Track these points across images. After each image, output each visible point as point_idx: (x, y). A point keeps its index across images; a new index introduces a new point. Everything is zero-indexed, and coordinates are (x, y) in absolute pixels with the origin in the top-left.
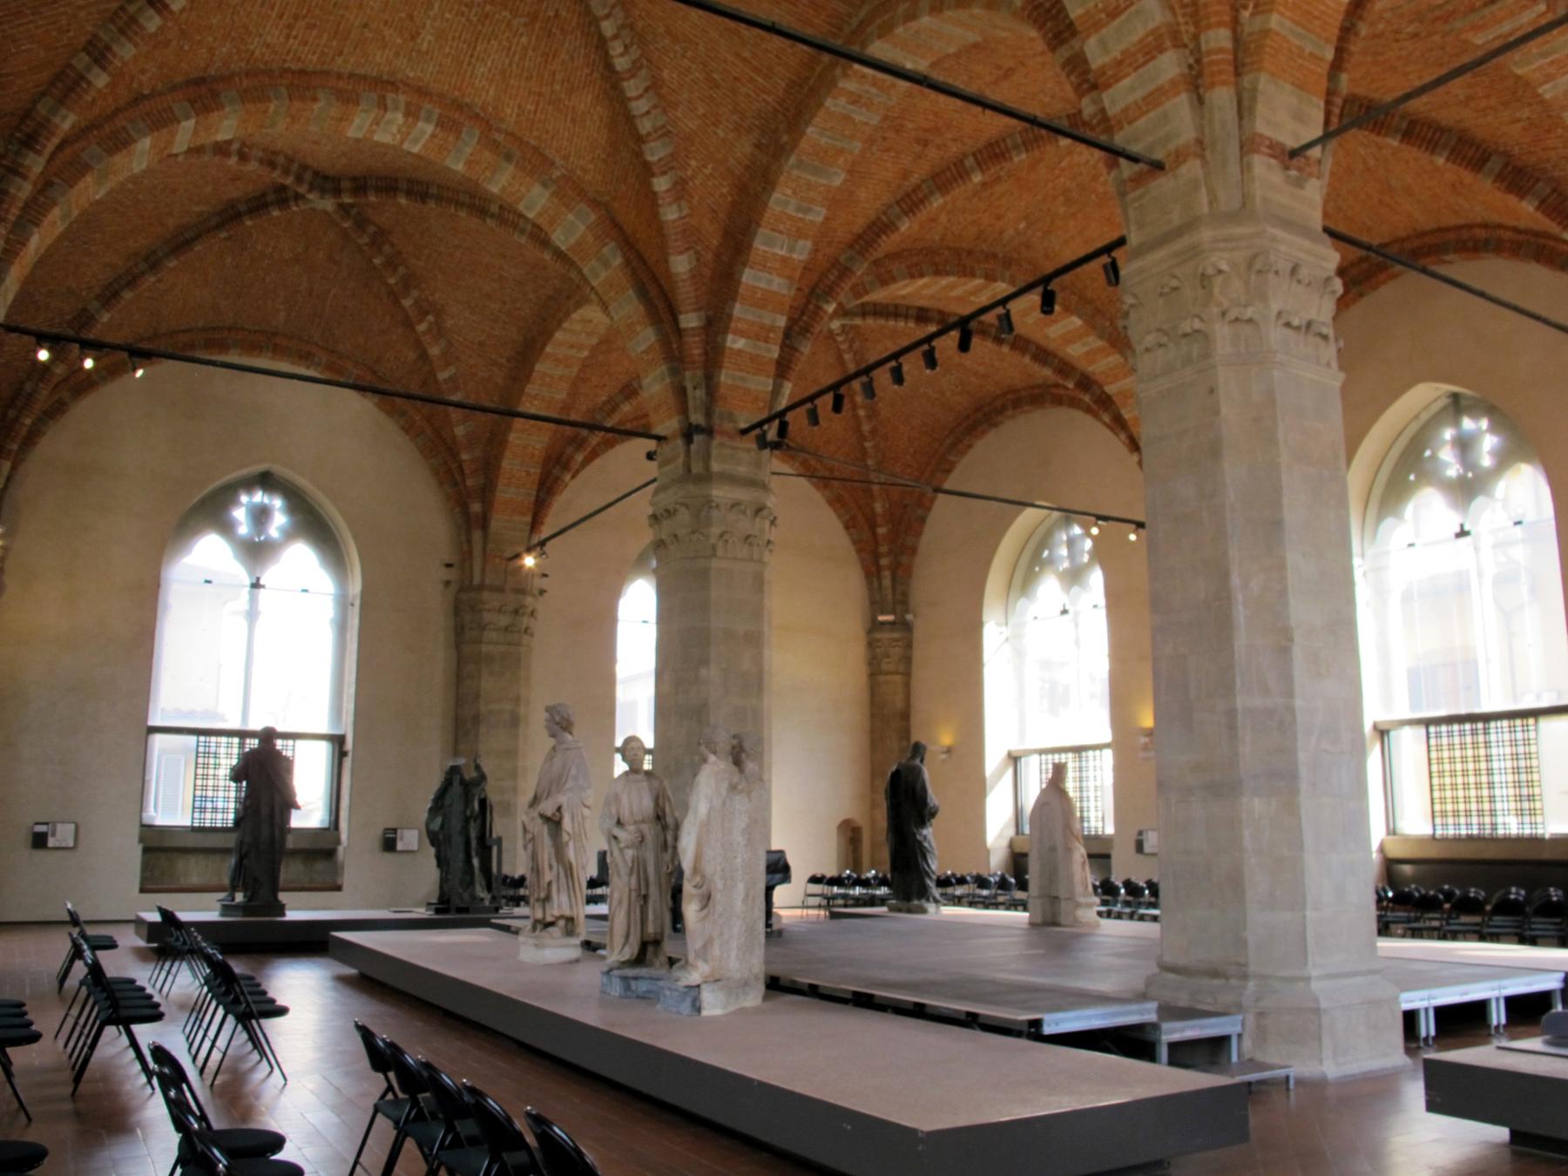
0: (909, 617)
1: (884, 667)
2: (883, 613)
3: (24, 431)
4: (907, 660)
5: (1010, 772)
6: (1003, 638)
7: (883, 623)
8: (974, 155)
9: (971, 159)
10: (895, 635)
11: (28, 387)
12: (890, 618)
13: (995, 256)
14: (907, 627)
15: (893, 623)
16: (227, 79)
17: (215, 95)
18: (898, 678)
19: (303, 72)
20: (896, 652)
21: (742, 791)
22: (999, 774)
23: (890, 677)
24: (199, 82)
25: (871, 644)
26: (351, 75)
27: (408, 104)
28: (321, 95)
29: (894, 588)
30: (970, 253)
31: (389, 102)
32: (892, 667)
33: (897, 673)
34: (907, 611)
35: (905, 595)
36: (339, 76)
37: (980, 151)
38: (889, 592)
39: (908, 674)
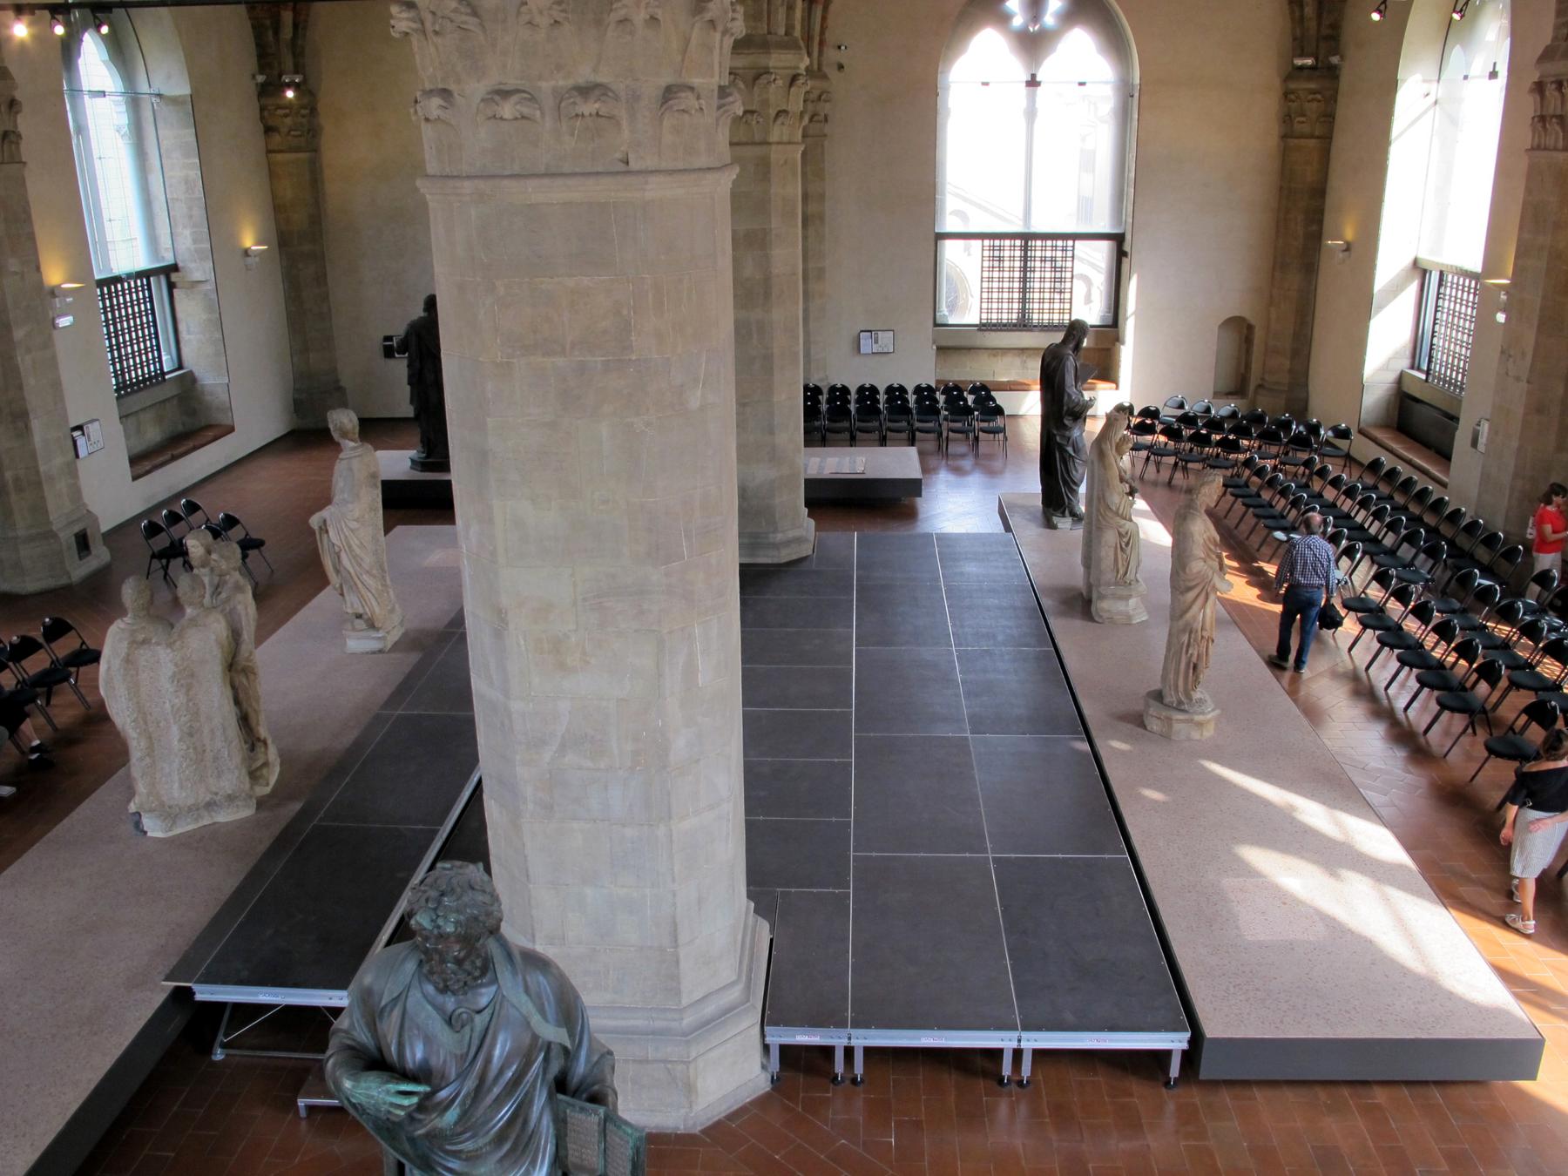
0: (1335, 60)
1: (1297, 127)
2: (1302, 55)
4: (1329, 118)
5: (1413, 287)
6: (1431, 99)
7: (1301, 68)
10: (1313, 86)
12: (1309, 62)
14: (1332, 73)
15: (1312, 68)
18: (1312, 143)
20: (1312, 108)
21: (158, 644)
22: (1396, 289)
23: (1303, 142)
25: (1286, 95)
29: (1319, 17)
32: (1306, 129)
33: (1312, 136)
34: (1336, 51)
35: (1336, 26)
38: (1312, 25)
39: (1327, 139)
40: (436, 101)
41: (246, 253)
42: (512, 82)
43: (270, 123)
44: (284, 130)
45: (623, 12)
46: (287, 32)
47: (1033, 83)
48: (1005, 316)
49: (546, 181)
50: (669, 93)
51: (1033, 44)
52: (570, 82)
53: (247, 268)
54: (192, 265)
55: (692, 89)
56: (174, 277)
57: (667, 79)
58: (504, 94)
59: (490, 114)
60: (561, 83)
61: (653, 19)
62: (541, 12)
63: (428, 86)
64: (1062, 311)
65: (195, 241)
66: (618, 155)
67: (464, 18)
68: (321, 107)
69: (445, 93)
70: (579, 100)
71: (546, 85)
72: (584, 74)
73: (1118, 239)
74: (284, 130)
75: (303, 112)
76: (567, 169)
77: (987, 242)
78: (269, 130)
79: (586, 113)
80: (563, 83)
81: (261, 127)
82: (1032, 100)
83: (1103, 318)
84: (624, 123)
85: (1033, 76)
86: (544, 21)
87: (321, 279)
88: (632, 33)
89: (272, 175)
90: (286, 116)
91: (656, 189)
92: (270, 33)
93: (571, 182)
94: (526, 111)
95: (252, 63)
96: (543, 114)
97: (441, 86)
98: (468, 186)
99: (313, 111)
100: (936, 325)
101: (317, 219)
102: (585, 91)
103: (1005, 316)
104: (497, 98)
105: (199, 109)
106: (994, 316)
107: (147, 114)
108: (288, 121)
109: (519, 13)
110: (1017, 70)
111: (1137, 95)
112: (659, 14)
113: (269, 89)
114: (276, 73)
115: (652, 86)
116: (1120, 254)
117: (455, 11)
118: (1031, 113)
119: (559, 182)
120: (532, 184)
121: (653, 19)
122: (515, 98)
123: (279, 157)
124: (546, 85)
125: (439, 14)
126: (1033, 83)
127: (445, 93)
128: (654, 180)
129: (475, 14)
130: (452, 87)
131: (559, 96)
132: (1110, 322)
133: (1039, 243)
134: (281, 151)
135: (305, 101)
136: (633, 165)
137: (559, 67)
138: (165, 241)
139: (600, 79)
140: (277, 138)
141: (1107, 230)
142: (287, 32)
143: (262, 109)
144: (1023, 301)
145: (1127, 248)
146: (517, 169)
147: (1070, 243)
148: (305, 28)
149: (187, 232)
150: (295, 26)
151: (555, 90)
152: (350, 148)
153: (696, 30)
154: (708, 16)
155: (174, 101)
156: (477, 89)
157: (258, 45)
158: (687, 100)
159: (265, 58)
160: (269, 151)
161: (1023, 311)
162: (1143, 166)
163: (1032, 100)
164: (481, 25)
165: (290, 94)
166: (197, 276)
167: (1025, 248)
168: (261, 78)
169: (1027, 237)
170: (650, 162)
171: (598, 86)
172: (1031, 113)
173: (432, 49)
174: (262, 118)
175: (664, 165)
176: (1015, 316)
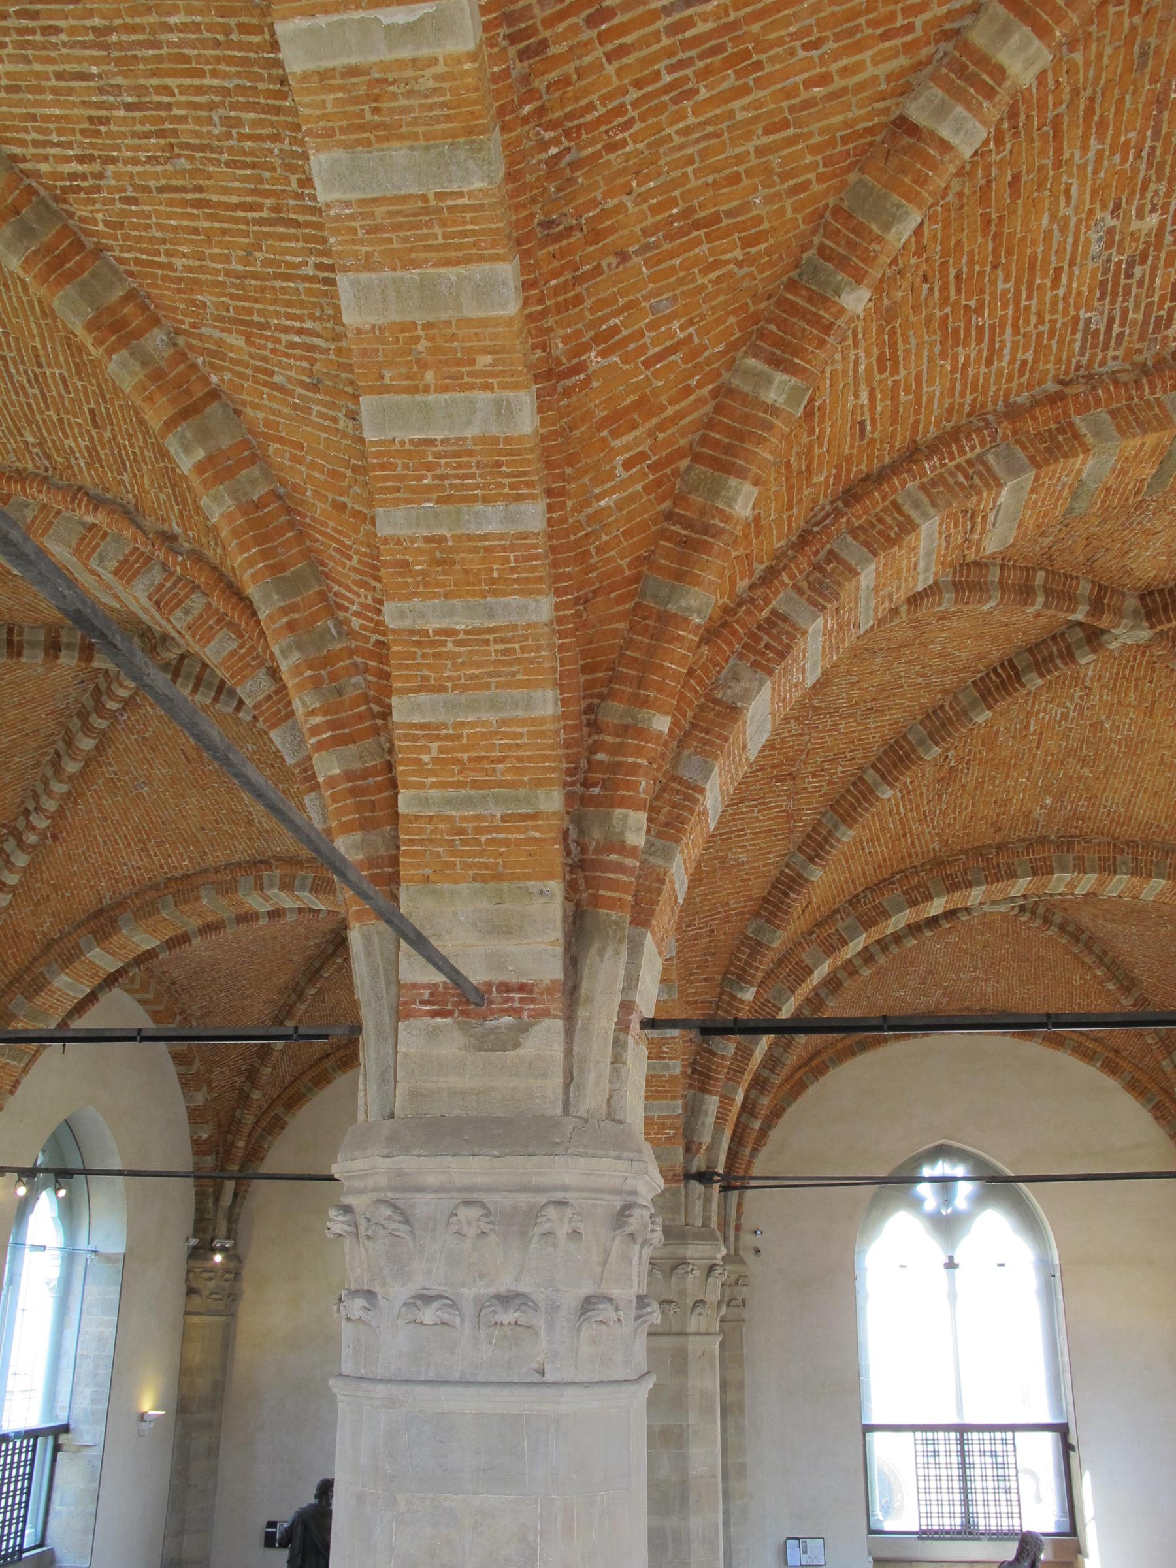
3: (240, 1154)
8: (874, 766)
9: (871, 771)
11: (238, 1114)
13: (1043, 840)
16: (120, 904)
17: (113, 921)
19: (186, 876)
24: (99, 913)
26: (227, 866)
27: (283, 876)
28: (203, 893)
30: (1000, 847)
31: (265, 881)
36: (217, 870)
37: (880, 759)
40: (360, 1302)
41: (142, 1417)
42: (435, 1289)
43: (194, 1285)
44: (206, 1293)
45: (547, 1226)
46: (227, 1200)
47: (951, 1265)
48: (947, 1522)
49: (460, 1389)
50: (588, 1304)
51: (947, 1226)
52: (492, 1290)
53: (140, 1434)
54: (84, 1427)
55: (610, 1300)
56: (63, 1439)
57: (586, 1289)
58: (426, 1299)
59: (411, 1318)
60: (483, 1291)
61: (576, 1233)
62: (469, 1224)
63: (353, 1286)
64: (1010, 1515)
65: (93, 1402)
66: (534, 1365)
67: (396, 1225)
68: (245, 1273)
69: (370, 1295)
70: (499, 1309)
71: (468, 1293)
72: (506, 1283)
73: (1062, 1430)
74: (206, 1293)
75: (227, 1276)
76: (481, 1377)
77: (919, 1435)
78: (191, 1291)
79: (505, 1322)
80: (486, 1290)
81: (184, 1289)
82: (952, 1280)
83: (1058, 1523)
84: (542, 1333)
85: (951, 1258)
86: (471, 1232)
87: (213, 1451)
88: (555, 1246)
89: (186, 1337)
90: (210, 1279)
91: (573, 1402)
92: (211, 1200)
93: (485, 1391)
94: (446, 1317)
95: (189, 1227)
96: (462, 1320)
97: (366, 1287)
98: (381, 1390)
99: (237, 1275)
100: (871, 1532)
101: (220, 1386)
102: (506, 1300)
103: (947, 1522)
104: (419, 1303)
105: (128, 1269)
106: (935, 1521)
107: (79, 1269)
108: (211, 1284)
109: (448, 1223)
110: (932, 1250)
111: (1058, 1275)
112: (581, 1227)
113: (200, 1251)
114: (209, 1237)
115: (571, 1298)
116: (1067, 1448)
117: (388, 1218)
118: (953, 1297)
119: (473, 1390)
120: (444, 1391)
121: (576, 1233)
122: (436, 1305)
123: (195, 1319)
124: (468, 1293)
125: (374, 1220)
126: (951, 1265)
127: (370, 1295)
128: (570, 1392)
129: (407, 1222)
130: (377, 1289)
131: (481, 1304)
132: (1066, 1529)
133: (975, 1435)
134: (198, 1314)
135: (232, 1265)
136: (549, 1377)
137: (482, 1276)
138: (64, 1399)
139: (521, 1288)
140: (197, 1300)
141: (1047, 1419)
142: (227, 1200)
143: (189, 1271)
144: (966, 1502)
145: (1072, 1440)
146: (431, 1376)
147: (1009, 1435)
148: (244, 1197)
149: (88, 1391)
150: (236, 1195)
151: (476, 1298)
152: (269, 1315)
153: (617, 1242)
154: (628, 1230)
155: (109, 1258)
156: (398, 1292)
157: (197, 1210)
158: (606, 1311)
159: (202, 1224)
160: (187, 1313)
161: (967, 1516)
162: (1076, 1352)
163: (952, 1280)
164: (412, 1233)
165: (218, 1258)
166: (87, 1439)
167: (961, 1442)
168: (193, 1242)
169: (962, 1429)
170: (567, 1376)
171: (518, 1295)
172: (953, 1297)
173: (362, 1251)
174: (187, 1280)
175: (580, 1377)
176: (958, 1522)
